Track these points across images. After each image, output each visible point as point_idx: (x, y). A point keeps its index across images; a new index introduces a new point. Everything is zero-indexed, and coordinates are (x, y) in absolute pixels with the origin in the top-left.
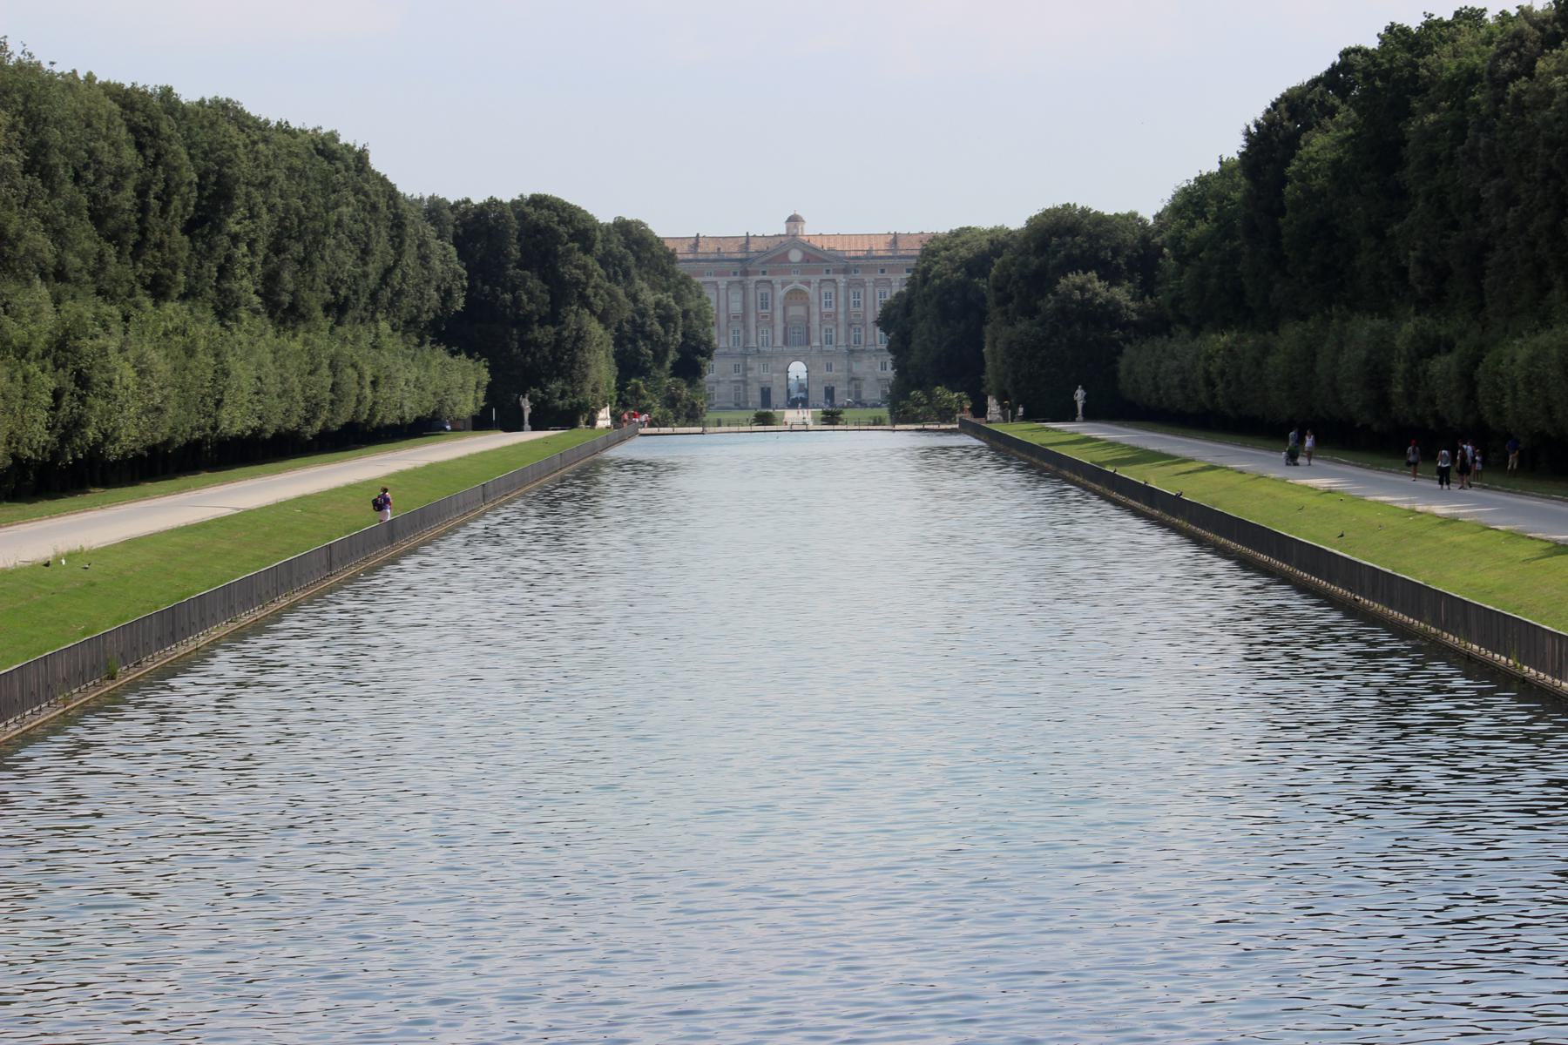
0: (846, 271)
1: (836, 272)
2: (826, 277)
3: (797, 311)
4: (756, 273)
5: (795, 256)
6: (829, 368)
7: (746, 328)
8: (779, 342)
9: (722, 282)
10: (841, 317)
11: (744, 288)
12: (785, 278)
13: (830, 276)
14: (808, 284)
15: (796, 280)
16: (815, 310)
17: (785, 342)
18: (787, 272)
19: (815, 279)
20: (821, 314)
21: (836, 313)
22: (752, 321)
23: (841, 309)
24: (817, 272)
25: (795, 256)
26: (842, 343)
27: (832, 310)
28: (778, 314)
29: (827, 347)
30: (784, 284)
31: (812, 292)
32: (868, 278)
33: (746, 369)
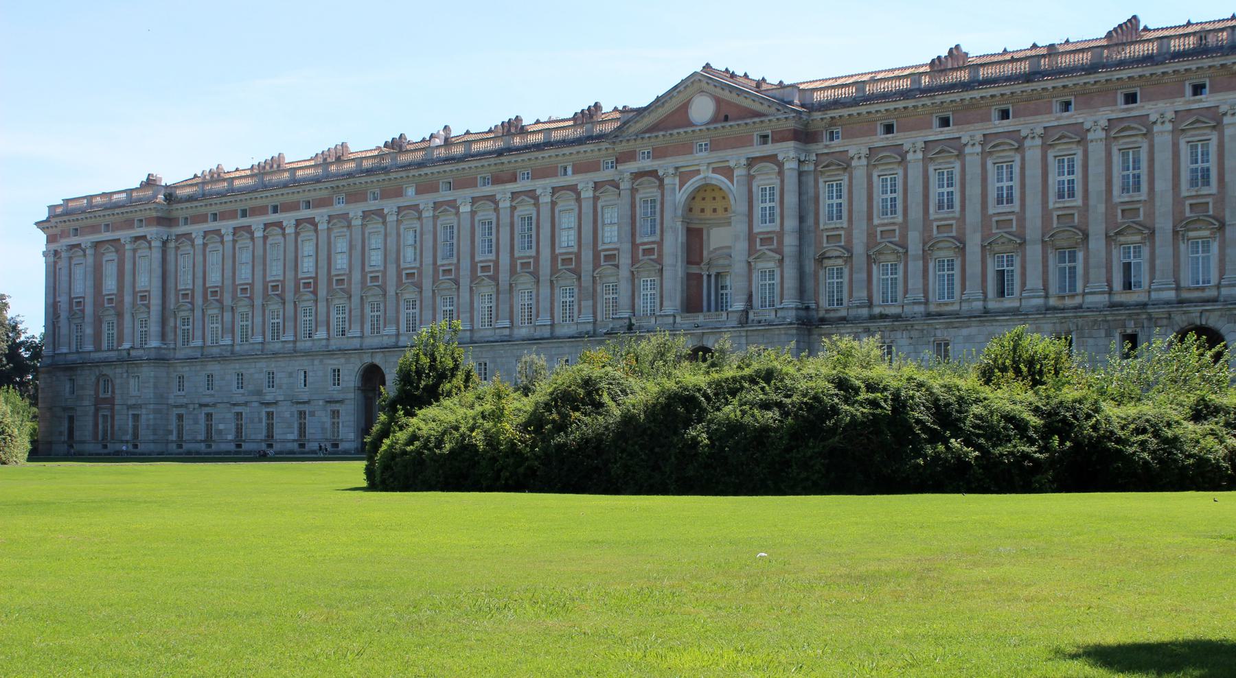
0: (804, 136)
1: (780, 137)
2: (758, 150)
10: (790, 241)
12: (680, 161)
13: (769, 149)
14: (728, 172)
15: (702, 164)
18: (685, 148)
19: (736, 158)
20: (751, 237)
21: (781, 234)
24: (741, 142)
27: (776, 226)
30: (684, 177)
32: (856, 148)
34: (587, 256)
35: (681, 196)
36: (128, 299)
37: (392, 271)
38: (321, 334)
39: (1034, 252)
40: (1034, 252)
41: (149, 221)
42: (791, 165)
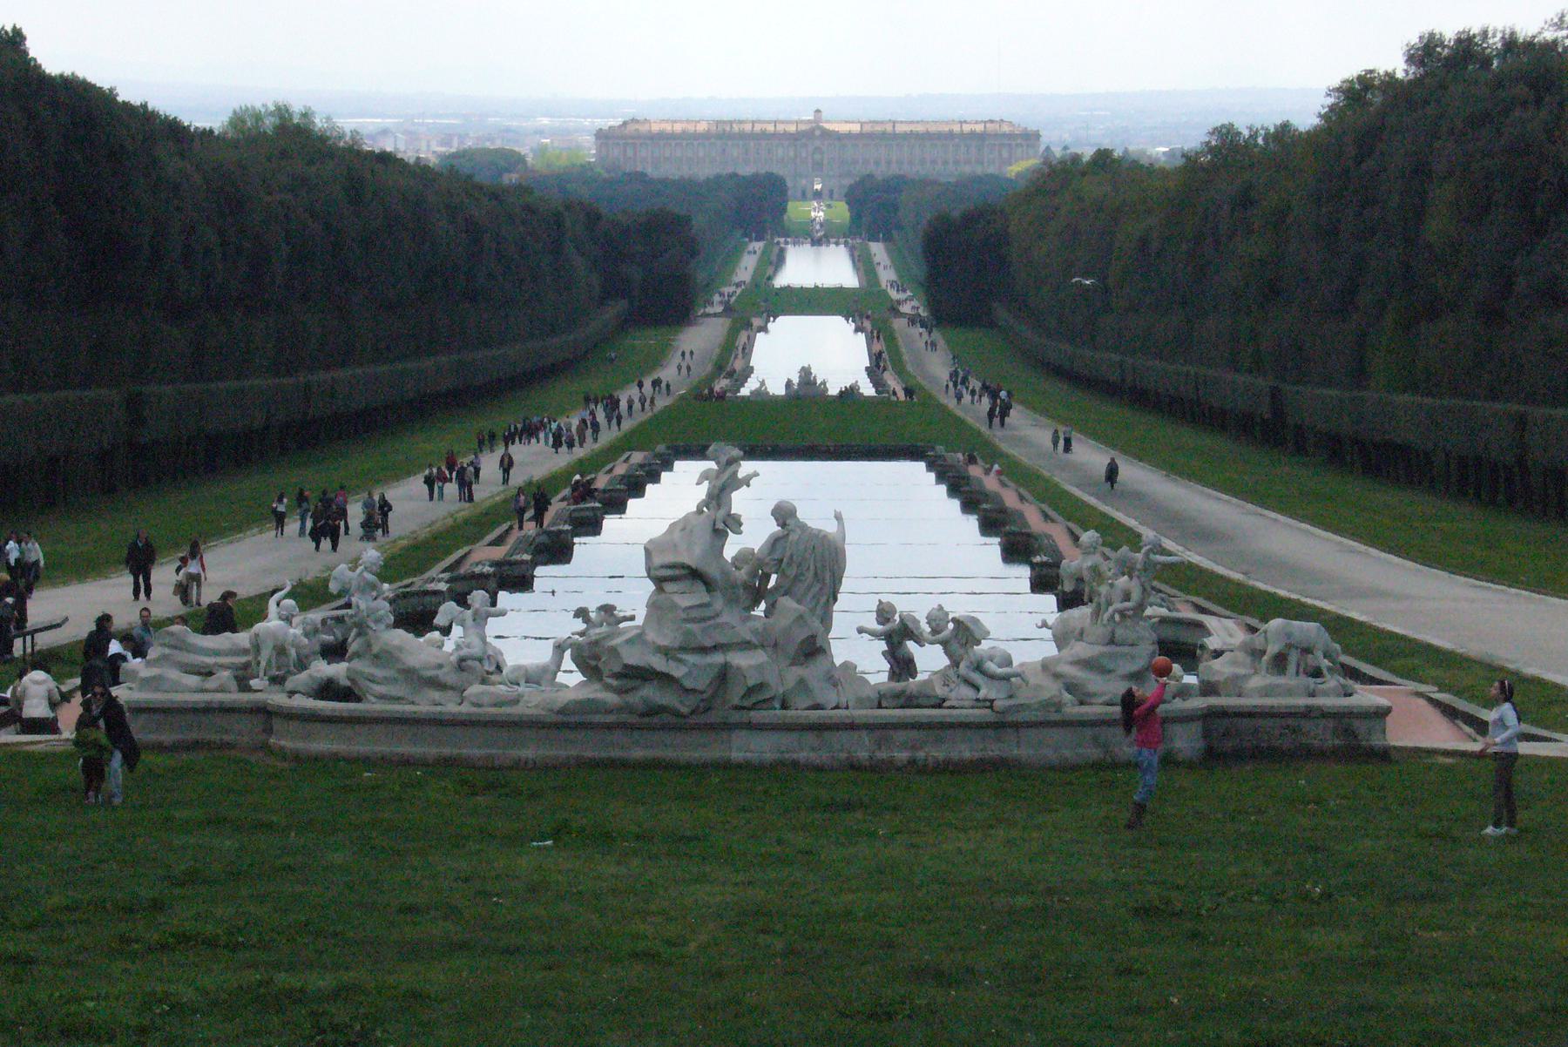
5: (818, 133)
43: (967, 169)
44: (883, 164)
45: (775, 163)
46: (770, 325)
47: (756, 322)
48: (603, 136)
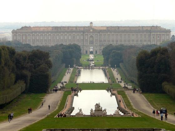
0: (99, 33)
1: (97, 33)
2: (96, 34)
3: (91, 39)
4: (85, 33)
5: (91, 30)
6: (96, 47)
7: (83, 41)
8: (89, 44)
9: (80, 34)
11: (83, 35)
14: (93, 35)
16: (94, 39)
17: (90, 44)
19: (94, 34)
22: (85, 40)
23: (98, 39)
25: (91, 30)
26: (98, 44)
28: (89, 39)
29: (96, 45)
30: (90, 35)
31: (94, 36)
33: (84, 48)
34: (80, 40)
35: (89, 36)
36: (27, 40)
37: (60, 39)
38: (52, 44)
39: (115, 42)
40: (115, 42)
41: (30, 33)
42: (98, 35)
43: (145, 43)
44: (115, 40)
45: (76, 40)
46: (79, 94)
47: (73, 94)
48: (14, 32)
